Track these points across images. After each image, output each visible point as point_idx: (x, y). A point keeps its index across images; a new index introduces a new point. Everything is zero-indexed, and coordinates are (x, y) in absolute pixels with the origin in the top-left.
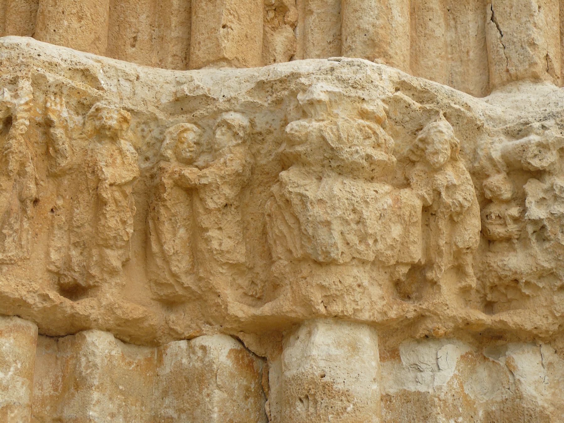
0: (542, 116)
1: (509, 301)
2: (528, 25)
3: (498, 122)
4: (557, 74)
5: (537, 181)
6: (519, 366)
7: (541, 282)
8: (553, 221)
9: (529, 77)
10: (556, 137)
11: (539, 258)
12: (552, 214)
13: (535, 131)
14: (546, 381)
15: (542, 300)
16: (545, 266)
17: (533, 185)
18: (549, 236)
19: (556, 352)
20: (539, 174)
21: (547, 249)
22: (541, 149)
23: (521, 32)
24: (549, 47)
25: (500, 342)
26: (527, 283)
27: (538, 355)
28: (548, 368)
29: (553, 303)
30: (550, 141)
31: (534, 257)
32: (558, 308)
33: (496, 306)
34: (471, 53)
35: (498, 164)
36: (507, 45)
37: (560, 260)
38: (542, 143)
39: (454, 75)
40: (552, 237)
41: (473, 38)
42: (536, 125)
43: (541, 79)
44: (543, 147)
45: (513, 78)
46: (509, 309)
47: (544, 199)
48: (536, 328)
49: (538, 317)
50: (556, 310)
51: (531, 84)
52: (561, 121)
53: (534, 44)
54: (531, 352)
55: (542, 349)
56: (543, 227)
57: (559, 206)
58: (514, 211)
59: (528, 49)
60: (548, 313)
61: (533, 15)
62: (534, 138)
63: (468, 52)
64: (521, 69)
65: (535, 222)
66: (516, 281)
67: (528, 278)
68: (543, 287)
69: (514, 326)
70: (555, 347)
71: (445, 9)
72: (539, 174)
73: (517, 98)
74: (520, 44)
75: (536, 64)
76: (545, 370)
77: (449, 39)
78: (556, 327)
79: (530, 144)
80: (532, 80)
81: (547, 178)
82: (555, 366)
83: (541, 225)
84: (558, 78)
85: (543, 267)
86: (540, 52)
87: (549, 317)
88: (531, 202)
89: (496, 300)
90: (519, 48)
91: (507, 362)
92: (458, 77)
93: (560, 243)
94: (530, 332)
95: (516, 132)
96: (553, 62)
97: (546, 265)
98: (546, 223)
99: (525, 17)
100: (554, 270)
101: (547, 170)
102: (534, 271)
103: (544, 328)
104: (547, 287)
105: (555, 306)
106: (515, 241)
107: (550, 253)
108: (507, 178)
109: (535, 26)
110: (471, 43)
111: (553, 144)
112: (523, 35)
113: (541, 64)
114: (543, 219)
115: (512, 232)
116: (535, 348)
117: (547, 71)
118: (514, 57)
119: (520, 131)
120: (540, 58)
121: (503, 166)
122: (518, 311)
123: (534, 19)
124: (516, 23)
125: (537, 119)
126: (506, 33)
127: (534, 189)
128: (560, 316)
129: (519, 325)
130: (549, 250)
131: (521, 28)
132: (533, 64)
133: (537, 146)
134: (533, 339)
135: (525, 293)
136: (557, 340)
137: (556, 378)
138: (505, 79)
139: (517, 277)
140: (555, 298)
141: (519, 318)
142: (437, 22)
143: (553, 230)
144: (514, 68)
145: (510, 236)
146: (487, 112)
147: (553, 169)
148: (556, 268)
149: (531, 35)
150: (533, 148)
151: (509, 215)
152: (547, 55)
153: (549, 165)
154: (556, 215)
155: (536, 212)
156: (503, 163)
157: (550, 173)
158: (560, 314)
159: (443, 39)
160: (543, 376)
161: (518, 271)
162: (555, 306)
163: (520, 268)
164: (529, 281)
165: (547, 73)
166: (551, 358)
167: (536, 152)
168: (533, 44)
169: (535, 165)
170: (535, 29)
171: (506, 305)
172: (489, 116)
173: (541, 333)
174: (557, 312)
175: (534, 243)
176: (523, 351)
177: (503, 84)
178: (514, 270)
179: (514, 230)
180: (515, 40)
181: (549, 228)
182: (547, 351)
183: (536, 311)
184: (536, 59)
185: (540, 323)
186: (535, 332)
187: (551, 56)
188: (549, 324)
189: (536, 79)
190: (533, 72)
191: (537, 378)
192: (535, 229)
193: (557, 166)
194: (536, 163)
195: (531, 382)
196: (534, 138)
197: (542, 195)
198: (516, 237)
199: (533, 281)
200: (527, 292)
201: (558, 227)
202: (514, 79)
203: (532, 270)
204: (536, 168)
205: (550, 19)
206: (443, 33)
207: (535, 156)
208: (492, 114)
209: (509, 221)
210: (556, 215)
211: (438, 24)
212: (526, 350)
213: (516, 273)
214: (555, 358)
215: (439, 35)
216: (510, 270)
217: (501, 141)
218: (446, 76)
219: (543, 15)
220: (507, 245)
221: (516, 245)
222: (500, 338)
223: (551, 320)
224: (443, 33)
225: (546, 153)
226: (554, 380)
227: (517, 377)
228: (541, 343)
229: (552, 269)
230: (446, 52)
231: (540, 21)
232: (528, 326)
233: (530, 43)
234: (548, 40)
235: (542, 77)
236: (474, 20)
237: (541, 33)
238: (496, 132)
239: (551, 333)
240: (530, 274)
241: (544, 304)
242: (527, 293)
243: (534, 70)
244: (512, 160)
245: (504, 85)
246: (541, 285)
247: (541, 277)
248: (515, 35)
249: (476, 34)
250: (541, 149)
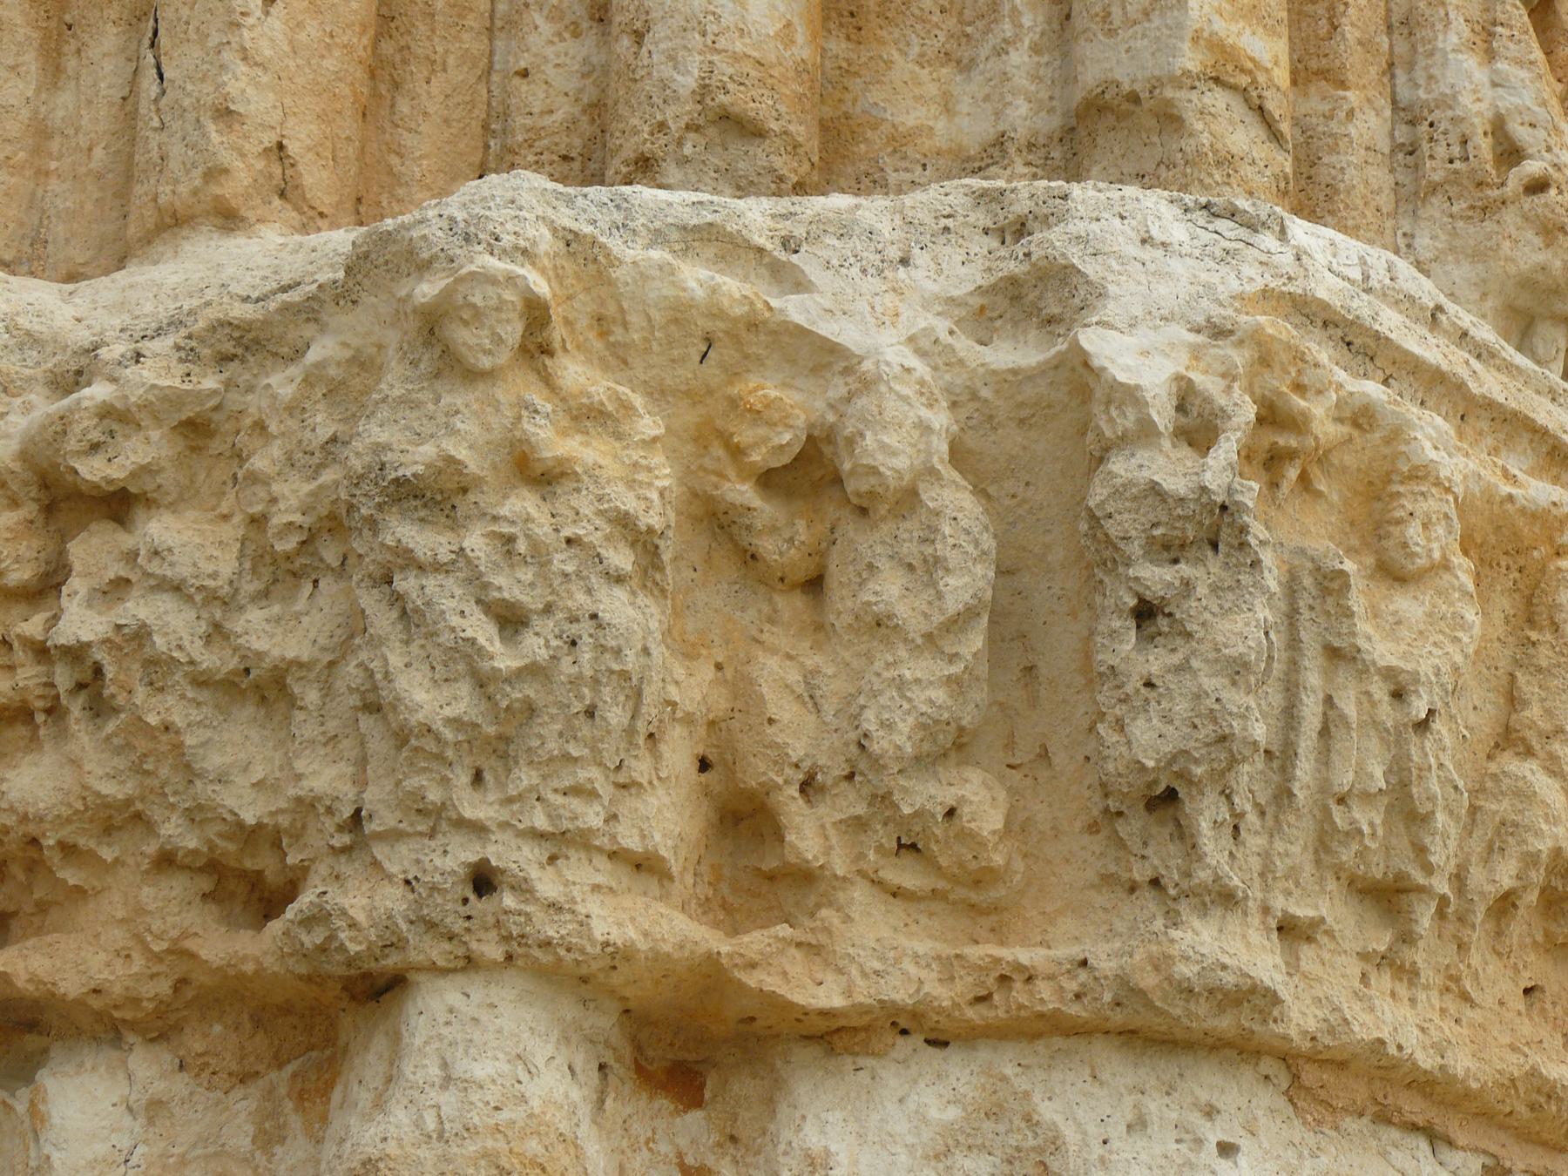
0: (154, 325)
1: (42, 908)
2: (227, 56)
3: (49, 350)
4: (316, 204)
5: (111, 525)
6: (54, 1114)
7: (109, 845)
8: (120, 649)
9: (208, 213)
10: (154, 386)
11: (87, 768)
12: (119, 627)
13: (106, 370)
14: (134, 1160)
15: (114, 905)
16: (104, 792)
17: (95, 541)
18: (113, 696)
19: (181, 1067)
20: (118, 505)
21: (108, 738)
22: (115, 427)
23: (203, 80)
24: (291, 122)
25: (32, 1041)
26: (68, 850)
27: (121, 1076)
28: (151, 1121)
29: (141, 911)
30: (133, 399)
31: (75, 763)
32: (157, 925)
33: (15, 925)
34: (98, 152)
35: (9, 478)
36: (167, 119)
37: (147, 773)
38: (112, 406)
39: (54, 220)
40: (121, 699)
41: (111, 104)
42: (116, 350)
43: (243, 220)
44: (116, 417)
45: (168, 220)
46: (39, 932)
47: (128, 581)
48: (95, 991)
49: (102, 956)
50: (149, 930)
51: (215, 236)
52: (190, 337)
53: (229, 112)
54: (102, 1069)
55: (131, 1058)
56: (98, 671)
57: (142, 602)
58: (33, 627)
59: (211, 128)
60: (130, 944)
61: (238, 25)
62: (98, 392)
63: (90, 149)
64: (183, 189)
65: (76, 653)
66: (34, 841)
67: (65, 833)
68: (116, 860)
69: (31, 987)
70: (181, 1053)
71: (53, 24)
72: (118, 505)
73: (140, 279)
74: (195, 115)
75: (226, 171)
76: (138, 1126)
77: (60, 113)
78: (164, 987)
79: (80, 409)
80: (219, 221)
81: (140, 513)
82: (177, 1111)
83: (89, 663)
84: (321, 215)
85: (98, 794)
86: (246, 137)
87: (134, 954)
88: (76, 593)
89: (12, 908)
90: (189, 128)
91: (32, 1101)
92: (61, 227)
93: (140, 719)
94: (79, 1002)
95: (71, 378)
96: (300, 168)
97: (109, 789)
98: (100, 655)
99: (219, 30)
100: (139, 806)
101: (133, 490)
102: (76, 812)
103: (117, 990)
104: (130, 861)
105: (148, 919)
106: (40, 718)
107: (118, 751)
108: (40, 522)
109: (244, 59)
110: (98, 121)
111: (145, 406)
112: (207, 88)
113: (244, 173)
114: (89, 645)
115: (26, 688)
116: (115, 1054)
117: (282, 194)
118: (176, 150)
119: (79, 373)
120: (243, 155)
121: (26, 484)
122: (49, 939)
123: (241, 36)
124: (197, 52)
125: (137, 336)
126: (172, 81)
127: (93, 552)
128: (169, 951)
129: (45, 984)
130: (115, 741)
131: (206, 66)
132: (216, 173)
133: (102, 417)
134: (103, 1026)
135: (65, 881)
136: (187, 1030)
137: (176, 1151)
138: (150, 225)
139: (32, 829)
140: (147, 893)
141: (47, 962)
142: (11, 62)
143: (122, 677)
144: (168, 189)
145: (24, 701)
146: (21, 320)
147: (151, 487)
148: (142, 799)
149: (225, 84)
150: (86, 423)
151: (18, 636)
152: (281, 146)
153: (133, 475)
154: (126, 630)
155: (80, 621)
156: (28, 475)
157: (149, 502)
158: (165, 945)
159: (25, 114)
160: (126, 1143)
161: (31, 810)
162: (148, 919)
163: (36, 803)
164: (71, 841)
165: (277, 202)
166: (159, 1088)
167: (95, 436)
168: (225, 114)
169: (88, 477)
170: (242, 68)
171: (37, 920)
172: (28, 334)
173: (116, 1007)
174: (156, 937)
175: (78, 721)
176: (81, 1065)
177: (147, 240)
178: (21, 809)
179: (31, 683)
180: (186, 102)
181: (110, 671)
182: (148, 1068)
183: (97, 936)
184: (227, 158)
185: (106, 975)
186: (96, 1003)
187: (293, 148)
188: (137, 977)
189: (229, 219)
190: (217, 198)
191: (101, 1149)
192: (78, 676)
193: (168, 478)
194: (93, 470)
195: (83, 1163)
196: (98, 392)
197: (116, 570)
198: (40, 704)
199: (81, 841)
200: (71, 876)
201: (136, 666)
202: (173, 223)
203: (70, 805)
204: (97, 486)
205: (312, 31)
206: (30, 93)
207: (95, 447)
208: (37, 327)
209: (20, 655)
210: (126, 630)
211: (13, 68)
212: (88, 1065)
213: (24, 818)
214: (181, 1085)
215: (11, 101)
216: (12, 809)
217: (28, 408)
218: (22, 225)
219: (277, 24)
220: (22, 730)
221: (42, 732)
222: (32, 1026)
223: (138, 964)
224: (30, 93)
225: (127, 437)
226: (164, 1155)
227: (47, 1149)
228: (131, 1038)
229: (129, 802)
230: (37, 151)
231: (264, 43)
232: (71, 986)
233: (218, 110)
234: (288, 101)
235: (243, 212)
236: (123, 50)
237: (265, 79)
238: (30, 379)
239: (150, 1006)
240: (69, 821)
241: (120, 914)
242: (71, 882)
243: (218, 191)
244: (45, 465)
245: (149, 242)
246: (107, 854)
247: (108, 830)
248: (189, 87)
249: (125, 92)
250: (115, 427)
